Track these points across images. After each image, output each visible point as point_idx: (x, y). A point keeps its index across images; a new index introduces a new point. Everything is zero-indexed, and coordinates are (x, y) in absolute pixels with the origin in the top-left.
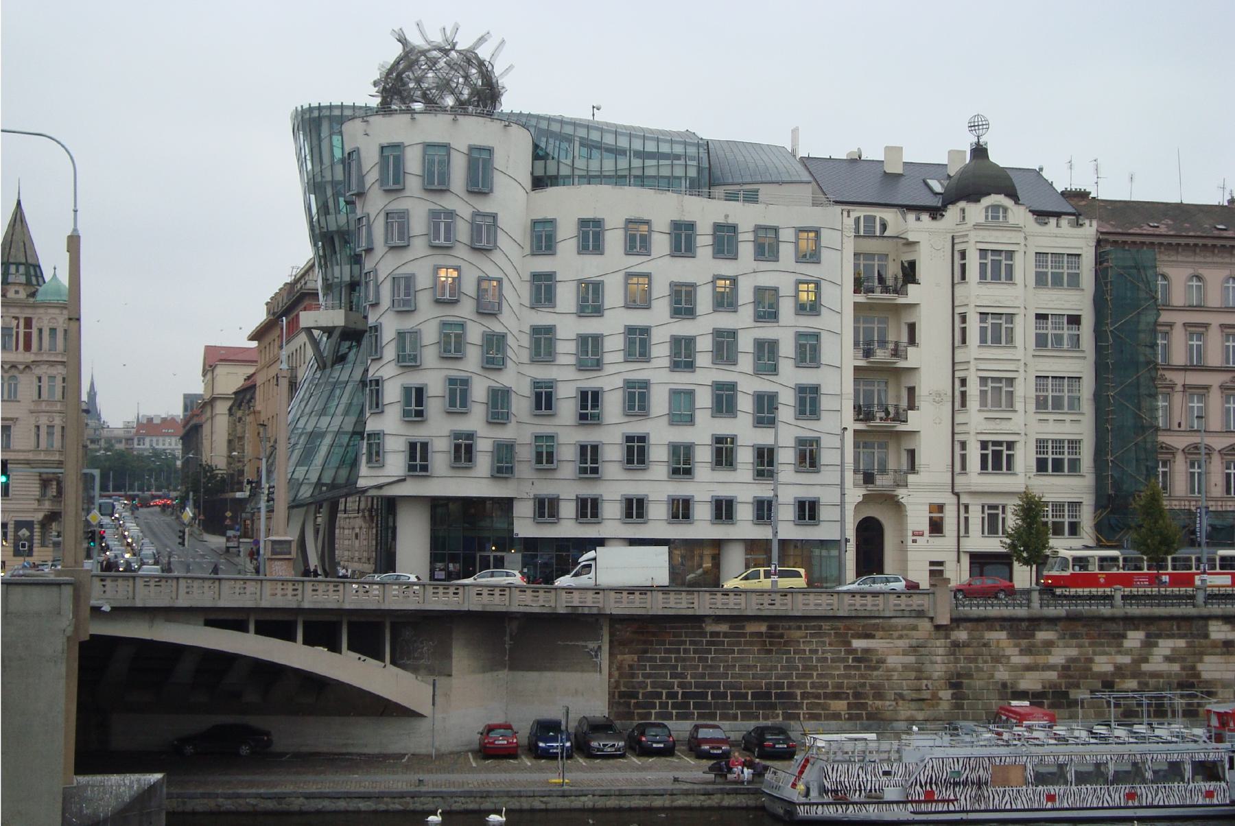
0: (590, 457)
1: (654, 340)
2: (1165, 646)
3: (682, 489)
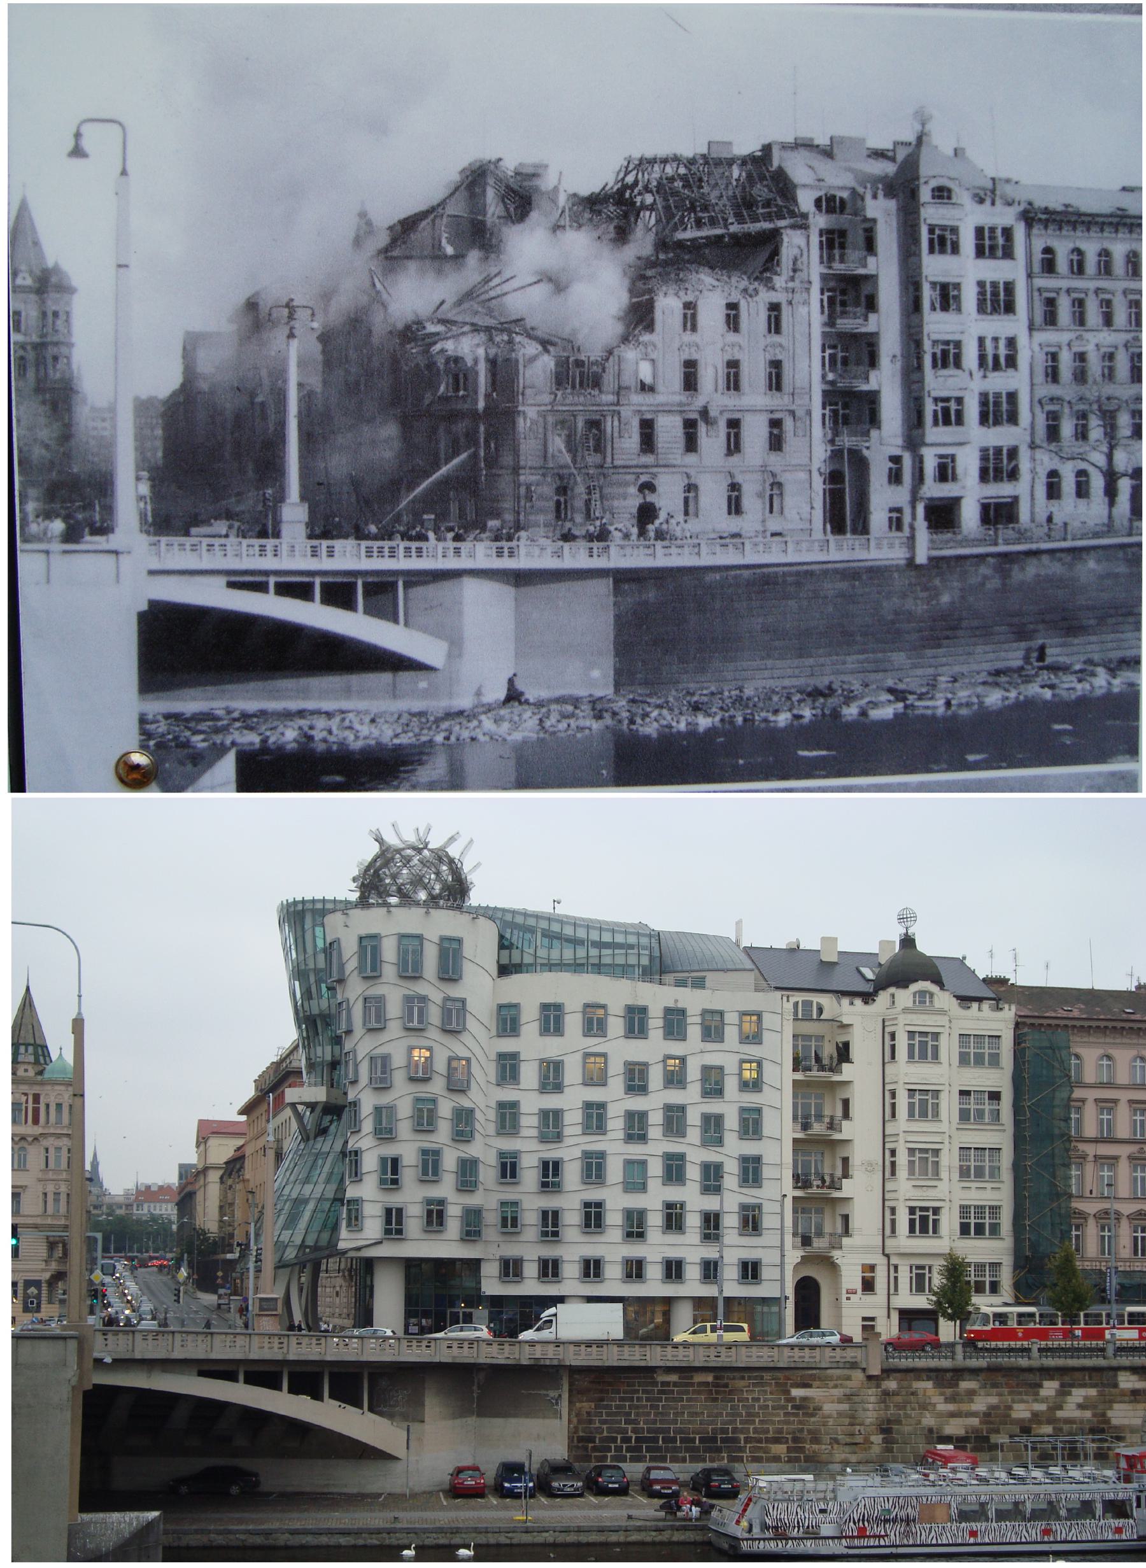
0: (551, 1222)
1: (610, 1114)
2: (1078, 1394)
3: (635, 1250)
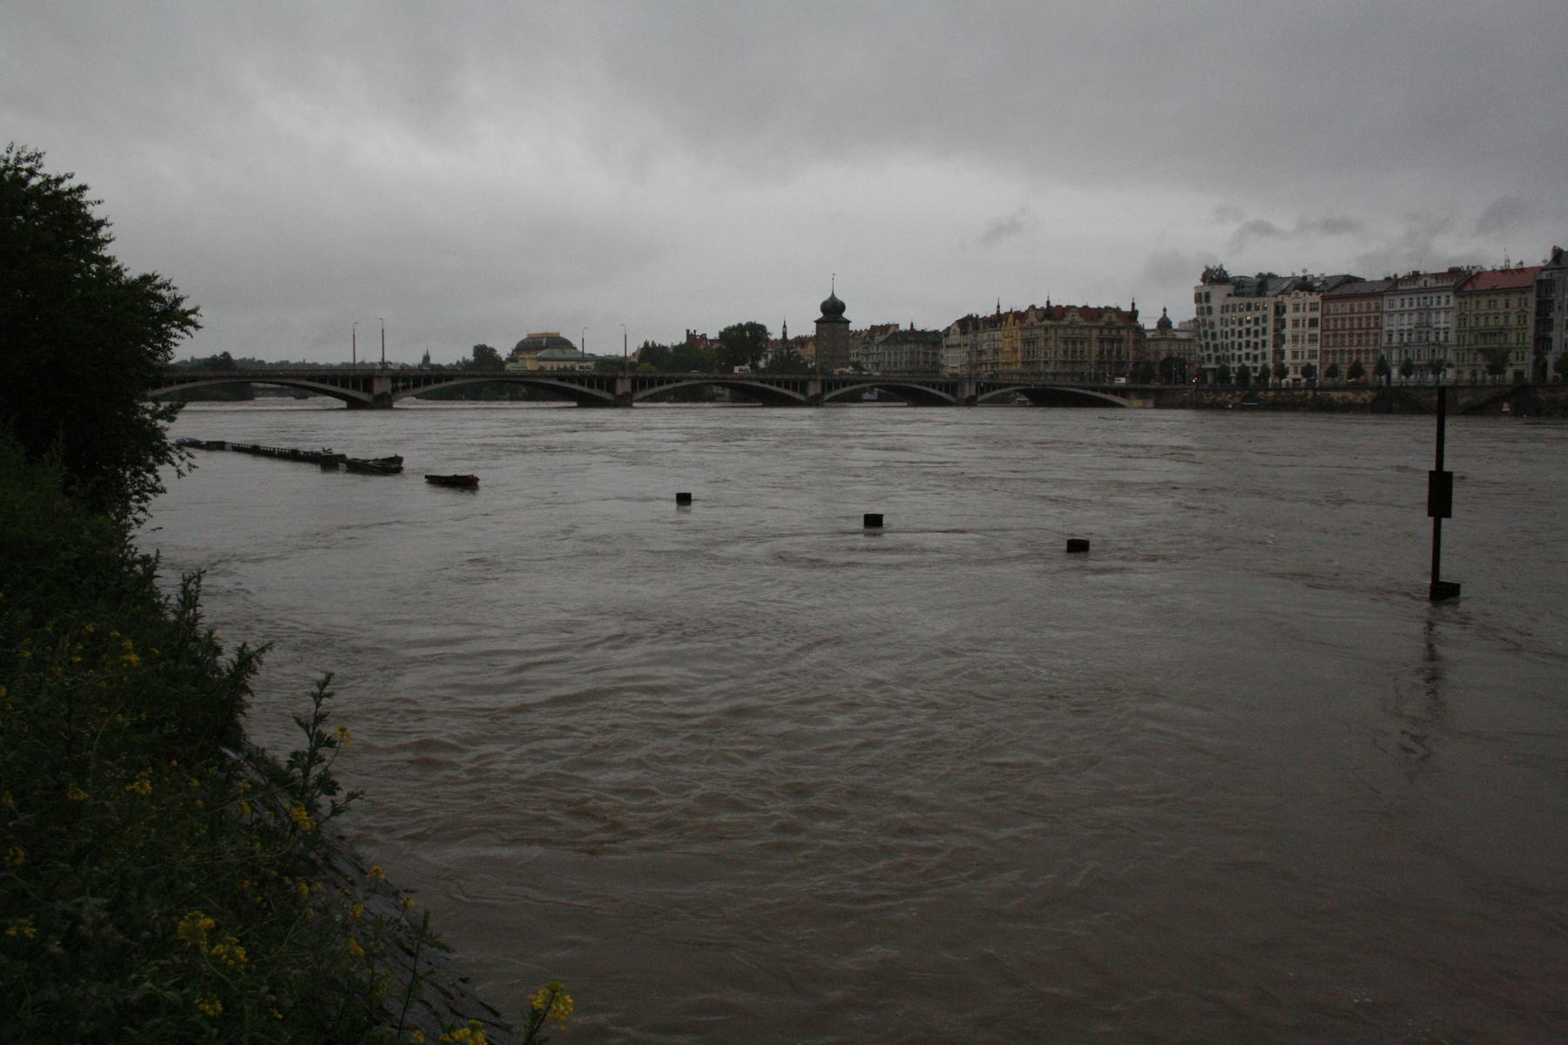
2: (1229, 396)
